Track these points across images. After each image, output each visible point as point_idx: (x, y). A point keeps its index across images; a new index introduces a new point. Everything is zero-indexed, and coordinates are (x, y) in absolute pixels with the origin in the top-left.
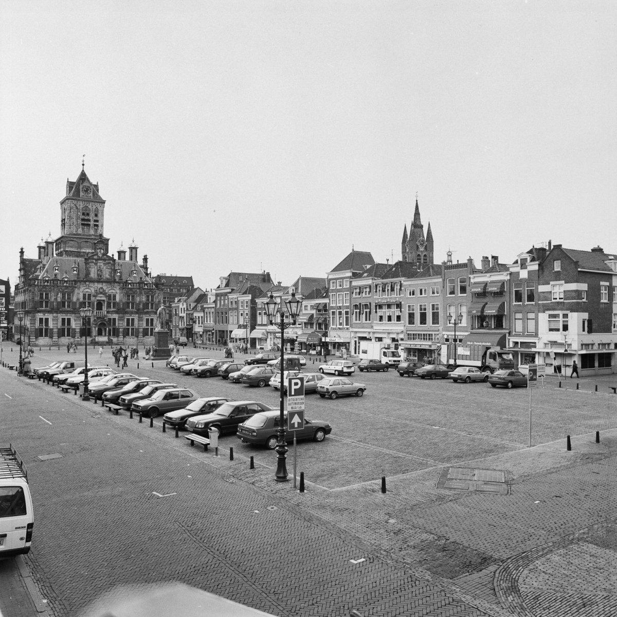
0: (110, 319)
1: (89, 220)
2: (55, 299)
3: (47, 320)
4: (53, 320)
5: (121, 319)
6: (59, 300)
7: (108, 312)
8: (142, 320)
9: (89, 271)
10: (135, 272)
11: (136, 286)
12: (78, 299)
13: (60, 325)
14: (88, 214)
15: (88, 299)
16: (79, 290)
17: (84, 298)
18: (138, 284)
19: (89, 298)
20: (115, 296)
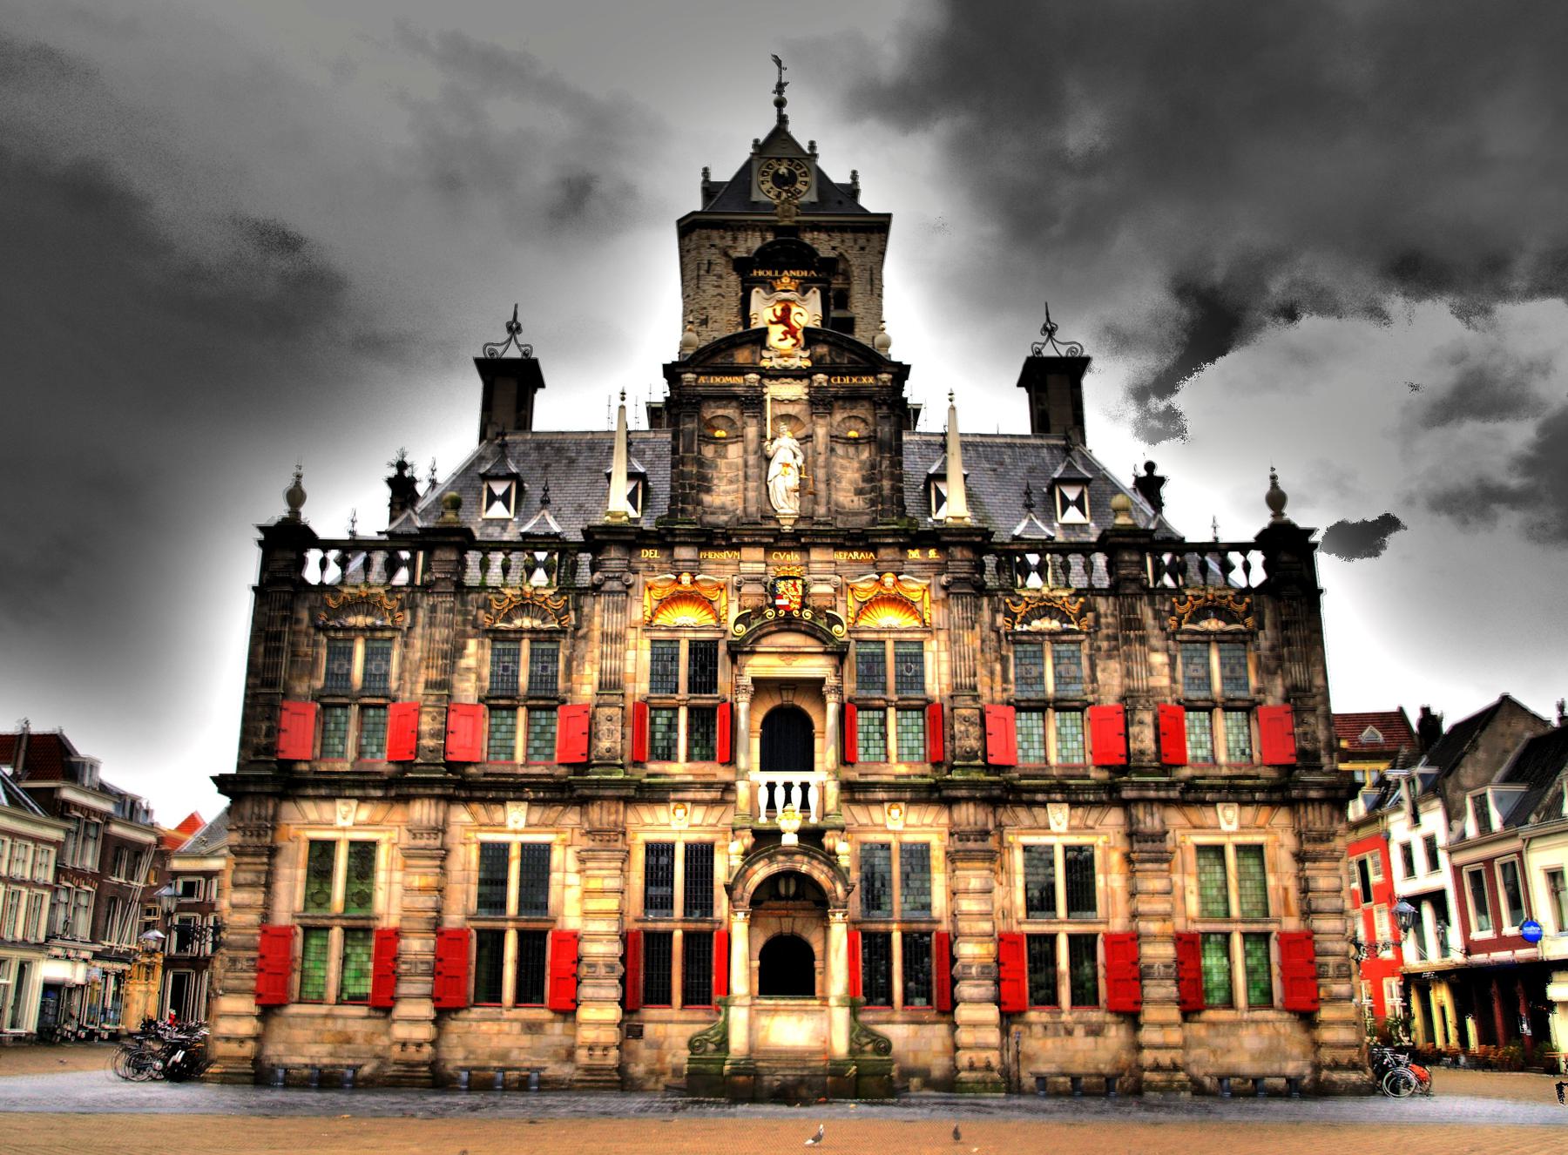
0: (871, 856)
2: (429, 685)
4: (409, 854)
5: (975, 848)
6: (468, 690)
7: (853, 792)
8: (1163, 858)
9: (701, 463)
10: (1072, 493)
11: (1089, 568)
12: (610, 686)
13: (461, 907)
15: (693, 687)
16: (622, 609)
18: (1100, 560)
19: (703, 677)
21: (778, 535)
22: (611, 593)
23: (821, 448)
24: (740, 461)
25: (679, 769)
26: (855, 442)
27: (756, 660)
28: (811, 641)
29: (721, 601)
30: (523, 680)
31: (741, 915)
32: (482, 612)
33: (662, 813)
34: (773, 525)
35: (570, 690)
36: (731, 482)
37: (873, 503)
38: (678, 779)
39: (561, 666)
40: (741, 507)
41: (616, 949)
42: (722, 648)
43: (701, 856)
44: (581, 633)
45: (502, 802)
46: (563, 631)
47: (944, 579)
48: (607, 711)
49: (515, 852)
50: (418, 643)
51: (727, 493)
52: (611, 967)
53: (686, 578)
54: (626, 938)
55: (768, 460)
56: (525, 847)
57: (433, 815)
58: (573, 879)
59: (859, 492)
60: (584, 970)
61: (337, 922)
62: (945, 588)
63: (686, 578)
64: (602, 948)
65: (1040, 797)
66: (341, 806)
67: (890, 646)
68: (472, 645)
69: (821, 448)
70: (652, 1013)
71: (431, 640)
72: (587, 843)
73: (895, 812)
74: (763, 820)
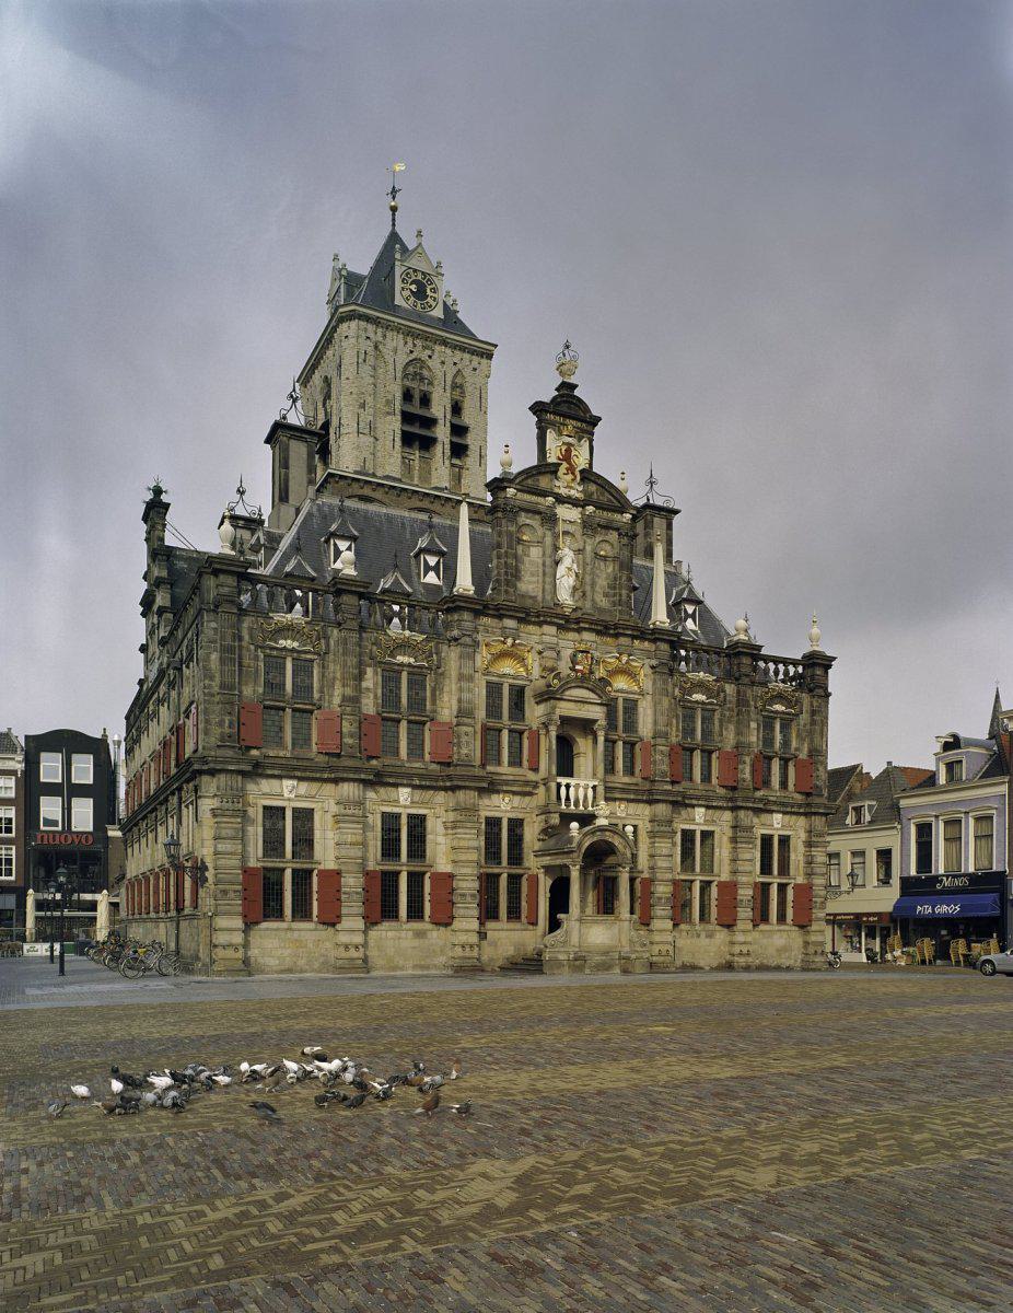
1: (430, 422)
2: (344, 699)
3: (304, 817)
4: (338, 819)
6: (369, 706)
14: (426, 400)
17: (493, 709)
20: (631, 707)
21: (567, 619)
22: (466, 645)
23: (588, 560)
24: (540, 561)
25: (505, 769)
26: (605, 558)
27: (563, 704)
28: (592, 695)
29: (531, 659)
30: (404, 700)
31: (578, 867)
32: (375, 648)
33: (496, 799)
34: (559, 611)
35: (435, 711)
36: (533, 575)
37: (614, 604)
38: (504, 777)
39: (428, 694)
40: (540, 594)
41: (476, 885)
42: (528, 693)
43: (516, 825)
44: (440, 671)
45: (396, 785)
46: (429, 668)
47: (654, 662)
48: (465, 729)
49: (404, 820)
50: (332, 667)
51: (530, 582)
52: (473, 896)
53: (510, 641)
54: (480, 877)
55: (557, 563)
56: (410, 816)
57: (356, 793)
58: (441, 839)
59: (606, 595)
60: (455, 899)
61: (289, 865)
62: (653, 667)
63: (510, 641)
64: (468, 885)
65: (694, 802)
66: (288, 783)
67: (620, 701)
68: (369, 671)
69: (588, 560)
70: (490, 925)
71: (345, 665)
72: (451, 816)
73: (623, 806)
74: (563, 807)
